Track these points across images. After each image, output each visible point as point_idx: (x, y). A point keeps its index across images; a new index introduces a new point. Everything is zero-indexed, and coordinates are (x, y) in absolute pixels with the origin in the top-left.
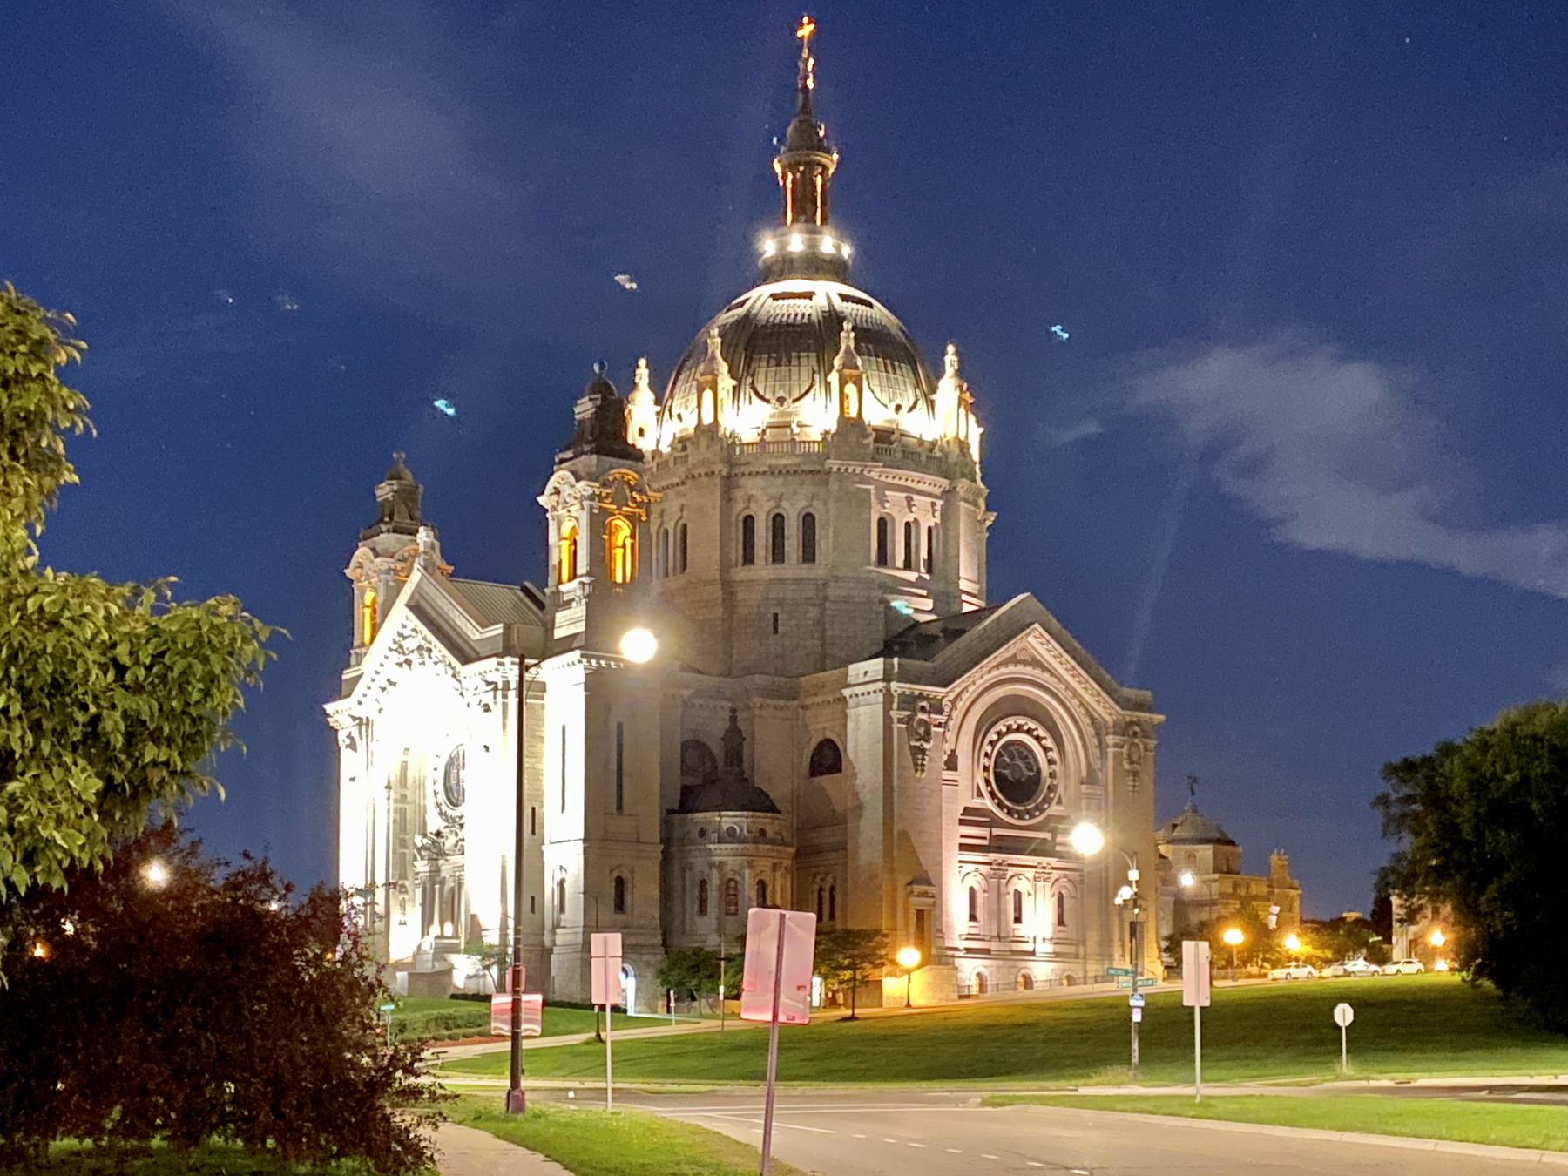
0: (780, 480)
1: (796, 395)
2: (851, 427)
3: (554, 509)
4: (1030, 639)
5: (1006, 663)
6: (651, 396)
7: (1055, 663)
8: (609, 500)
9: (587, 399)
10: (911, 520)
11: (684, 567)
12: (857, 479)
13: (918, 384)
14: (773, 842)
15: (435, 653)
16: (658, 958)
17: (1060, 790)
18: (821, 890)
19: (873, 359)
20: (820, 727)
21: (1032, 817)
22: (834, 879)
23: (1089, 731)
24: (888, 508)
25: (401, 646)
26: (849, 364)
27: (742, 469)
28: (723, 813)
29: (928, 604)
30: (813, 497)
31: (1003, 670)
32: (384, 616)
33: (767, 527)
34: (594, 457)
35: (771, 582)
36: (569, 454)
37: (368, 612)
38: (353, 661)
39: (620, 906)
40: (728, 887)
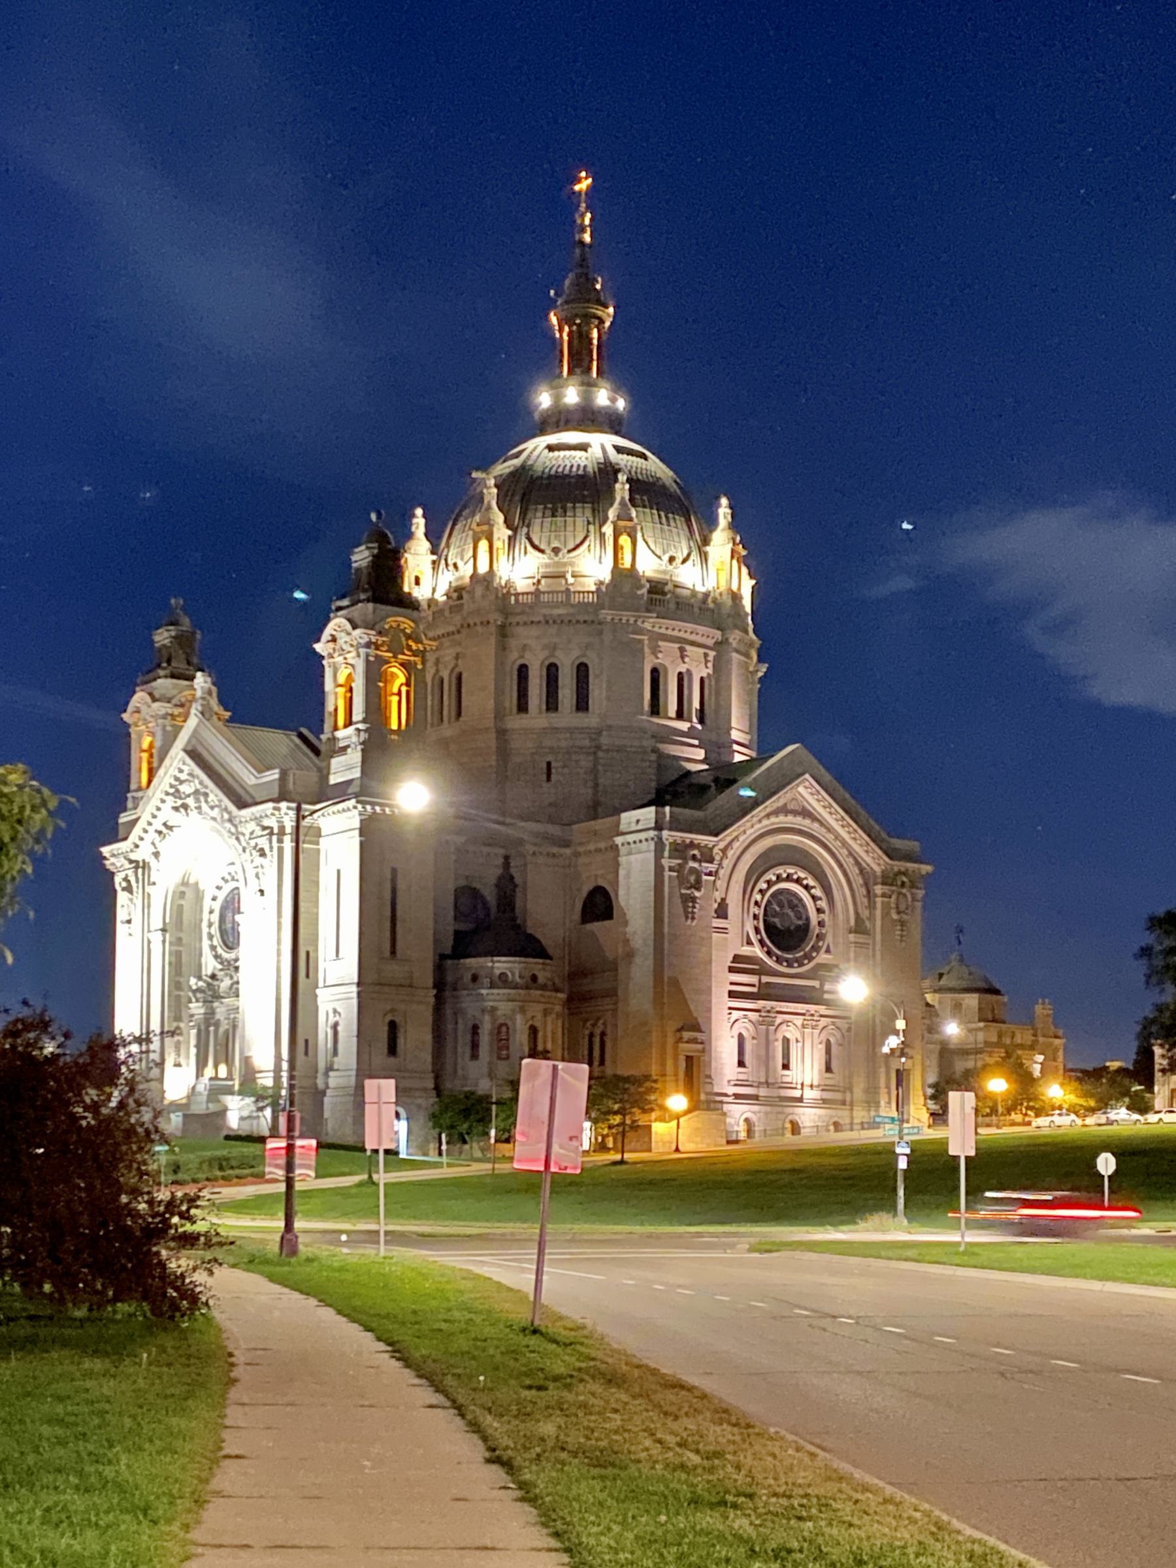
0: (553, 630)
1: (571, 546)
2: (624, 577)
3: (331, 656)
4: (801, 789)
5: (776, 813)
6: (426, 545)
7: (825, 814)
8: (385, 648)
9: (363, 547)
10: (684, 670)
11: (459, 714)
14: (544, 988)
15: (211, 797)
17: (829, 939)
18: (591, 1035)
19: (647, 510)
20: (591, 876)
21: (801, 965)
22: (604, 1024)
23: (858, 881)
24: (662, 659)
25: (177, 791)
26: (623, 516)
27: (518, 619)
28: (495, 959)
29: (700, 754)
30: (587, 647)
31: (773, 819)
32: (161, 761)
33: (541, 676)
34: (370, 606)
36: (345, 602)
37: (145, 756)
38: (130, 804)
39: (392, 1050)
40: (499, 1032)
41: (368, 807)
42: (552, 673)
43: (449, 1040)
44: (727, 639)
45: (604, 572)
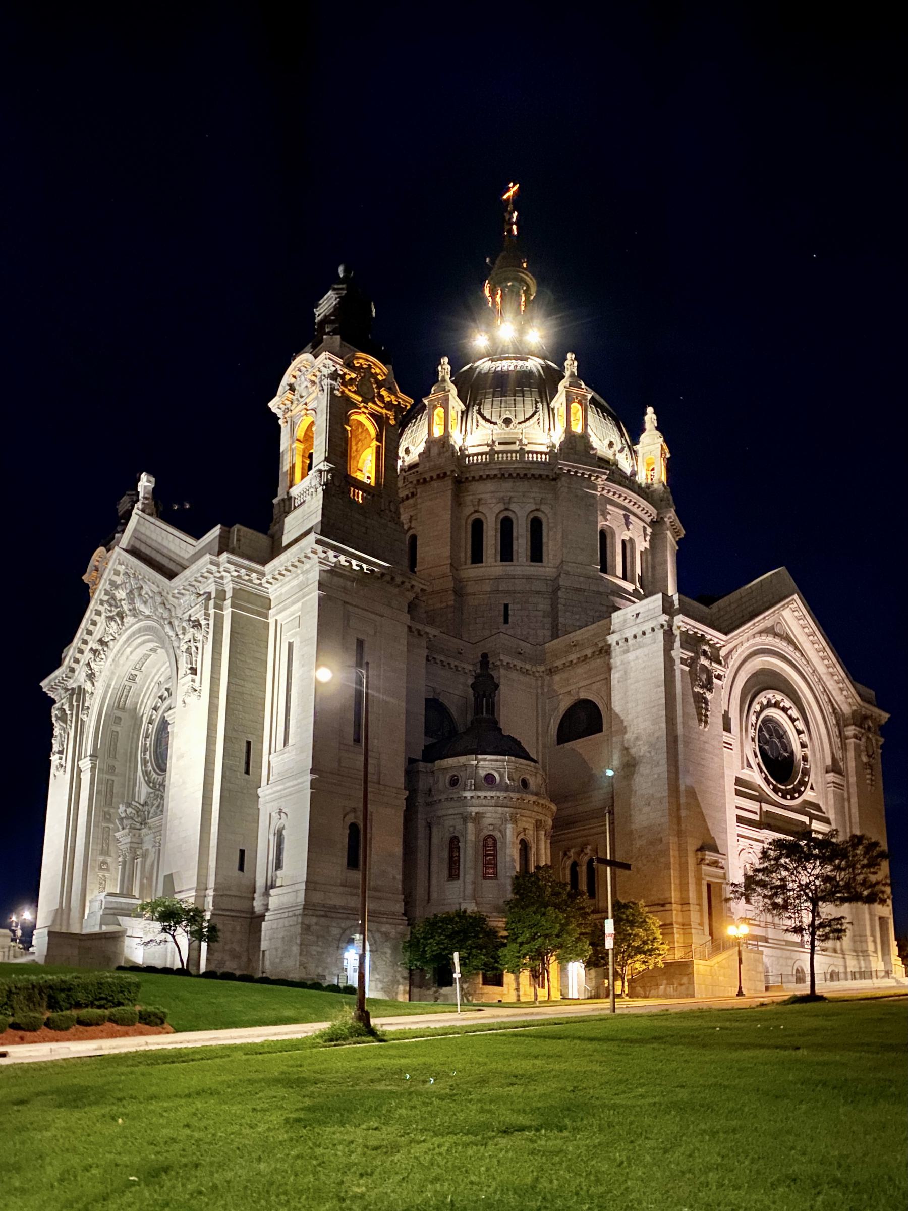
0: (508, 485)
10: (627, 539)
12: (585, 484)
13: (622, 436)
16: (401, 928)
28: (480, 757)
33: (496, 529)
35: (498, 579)
39: (353, 862)
41: (331, 553)
42: (506, 526)
43: (421, 857)
44: (662, 518)
45: (558, 437)
